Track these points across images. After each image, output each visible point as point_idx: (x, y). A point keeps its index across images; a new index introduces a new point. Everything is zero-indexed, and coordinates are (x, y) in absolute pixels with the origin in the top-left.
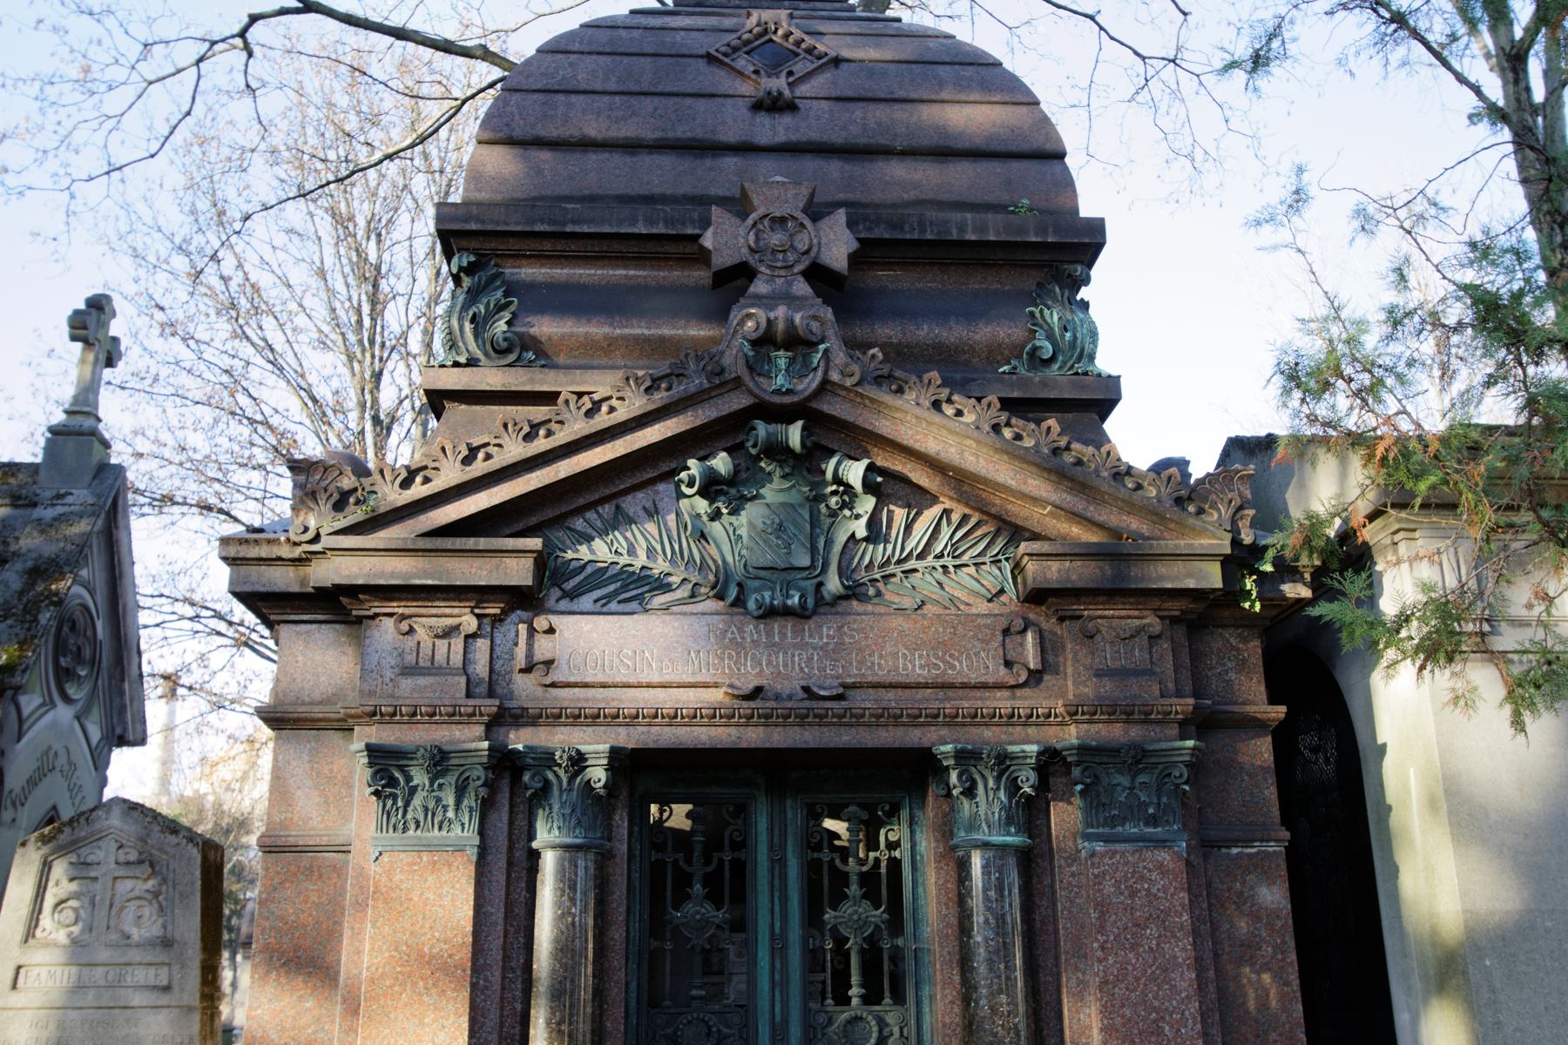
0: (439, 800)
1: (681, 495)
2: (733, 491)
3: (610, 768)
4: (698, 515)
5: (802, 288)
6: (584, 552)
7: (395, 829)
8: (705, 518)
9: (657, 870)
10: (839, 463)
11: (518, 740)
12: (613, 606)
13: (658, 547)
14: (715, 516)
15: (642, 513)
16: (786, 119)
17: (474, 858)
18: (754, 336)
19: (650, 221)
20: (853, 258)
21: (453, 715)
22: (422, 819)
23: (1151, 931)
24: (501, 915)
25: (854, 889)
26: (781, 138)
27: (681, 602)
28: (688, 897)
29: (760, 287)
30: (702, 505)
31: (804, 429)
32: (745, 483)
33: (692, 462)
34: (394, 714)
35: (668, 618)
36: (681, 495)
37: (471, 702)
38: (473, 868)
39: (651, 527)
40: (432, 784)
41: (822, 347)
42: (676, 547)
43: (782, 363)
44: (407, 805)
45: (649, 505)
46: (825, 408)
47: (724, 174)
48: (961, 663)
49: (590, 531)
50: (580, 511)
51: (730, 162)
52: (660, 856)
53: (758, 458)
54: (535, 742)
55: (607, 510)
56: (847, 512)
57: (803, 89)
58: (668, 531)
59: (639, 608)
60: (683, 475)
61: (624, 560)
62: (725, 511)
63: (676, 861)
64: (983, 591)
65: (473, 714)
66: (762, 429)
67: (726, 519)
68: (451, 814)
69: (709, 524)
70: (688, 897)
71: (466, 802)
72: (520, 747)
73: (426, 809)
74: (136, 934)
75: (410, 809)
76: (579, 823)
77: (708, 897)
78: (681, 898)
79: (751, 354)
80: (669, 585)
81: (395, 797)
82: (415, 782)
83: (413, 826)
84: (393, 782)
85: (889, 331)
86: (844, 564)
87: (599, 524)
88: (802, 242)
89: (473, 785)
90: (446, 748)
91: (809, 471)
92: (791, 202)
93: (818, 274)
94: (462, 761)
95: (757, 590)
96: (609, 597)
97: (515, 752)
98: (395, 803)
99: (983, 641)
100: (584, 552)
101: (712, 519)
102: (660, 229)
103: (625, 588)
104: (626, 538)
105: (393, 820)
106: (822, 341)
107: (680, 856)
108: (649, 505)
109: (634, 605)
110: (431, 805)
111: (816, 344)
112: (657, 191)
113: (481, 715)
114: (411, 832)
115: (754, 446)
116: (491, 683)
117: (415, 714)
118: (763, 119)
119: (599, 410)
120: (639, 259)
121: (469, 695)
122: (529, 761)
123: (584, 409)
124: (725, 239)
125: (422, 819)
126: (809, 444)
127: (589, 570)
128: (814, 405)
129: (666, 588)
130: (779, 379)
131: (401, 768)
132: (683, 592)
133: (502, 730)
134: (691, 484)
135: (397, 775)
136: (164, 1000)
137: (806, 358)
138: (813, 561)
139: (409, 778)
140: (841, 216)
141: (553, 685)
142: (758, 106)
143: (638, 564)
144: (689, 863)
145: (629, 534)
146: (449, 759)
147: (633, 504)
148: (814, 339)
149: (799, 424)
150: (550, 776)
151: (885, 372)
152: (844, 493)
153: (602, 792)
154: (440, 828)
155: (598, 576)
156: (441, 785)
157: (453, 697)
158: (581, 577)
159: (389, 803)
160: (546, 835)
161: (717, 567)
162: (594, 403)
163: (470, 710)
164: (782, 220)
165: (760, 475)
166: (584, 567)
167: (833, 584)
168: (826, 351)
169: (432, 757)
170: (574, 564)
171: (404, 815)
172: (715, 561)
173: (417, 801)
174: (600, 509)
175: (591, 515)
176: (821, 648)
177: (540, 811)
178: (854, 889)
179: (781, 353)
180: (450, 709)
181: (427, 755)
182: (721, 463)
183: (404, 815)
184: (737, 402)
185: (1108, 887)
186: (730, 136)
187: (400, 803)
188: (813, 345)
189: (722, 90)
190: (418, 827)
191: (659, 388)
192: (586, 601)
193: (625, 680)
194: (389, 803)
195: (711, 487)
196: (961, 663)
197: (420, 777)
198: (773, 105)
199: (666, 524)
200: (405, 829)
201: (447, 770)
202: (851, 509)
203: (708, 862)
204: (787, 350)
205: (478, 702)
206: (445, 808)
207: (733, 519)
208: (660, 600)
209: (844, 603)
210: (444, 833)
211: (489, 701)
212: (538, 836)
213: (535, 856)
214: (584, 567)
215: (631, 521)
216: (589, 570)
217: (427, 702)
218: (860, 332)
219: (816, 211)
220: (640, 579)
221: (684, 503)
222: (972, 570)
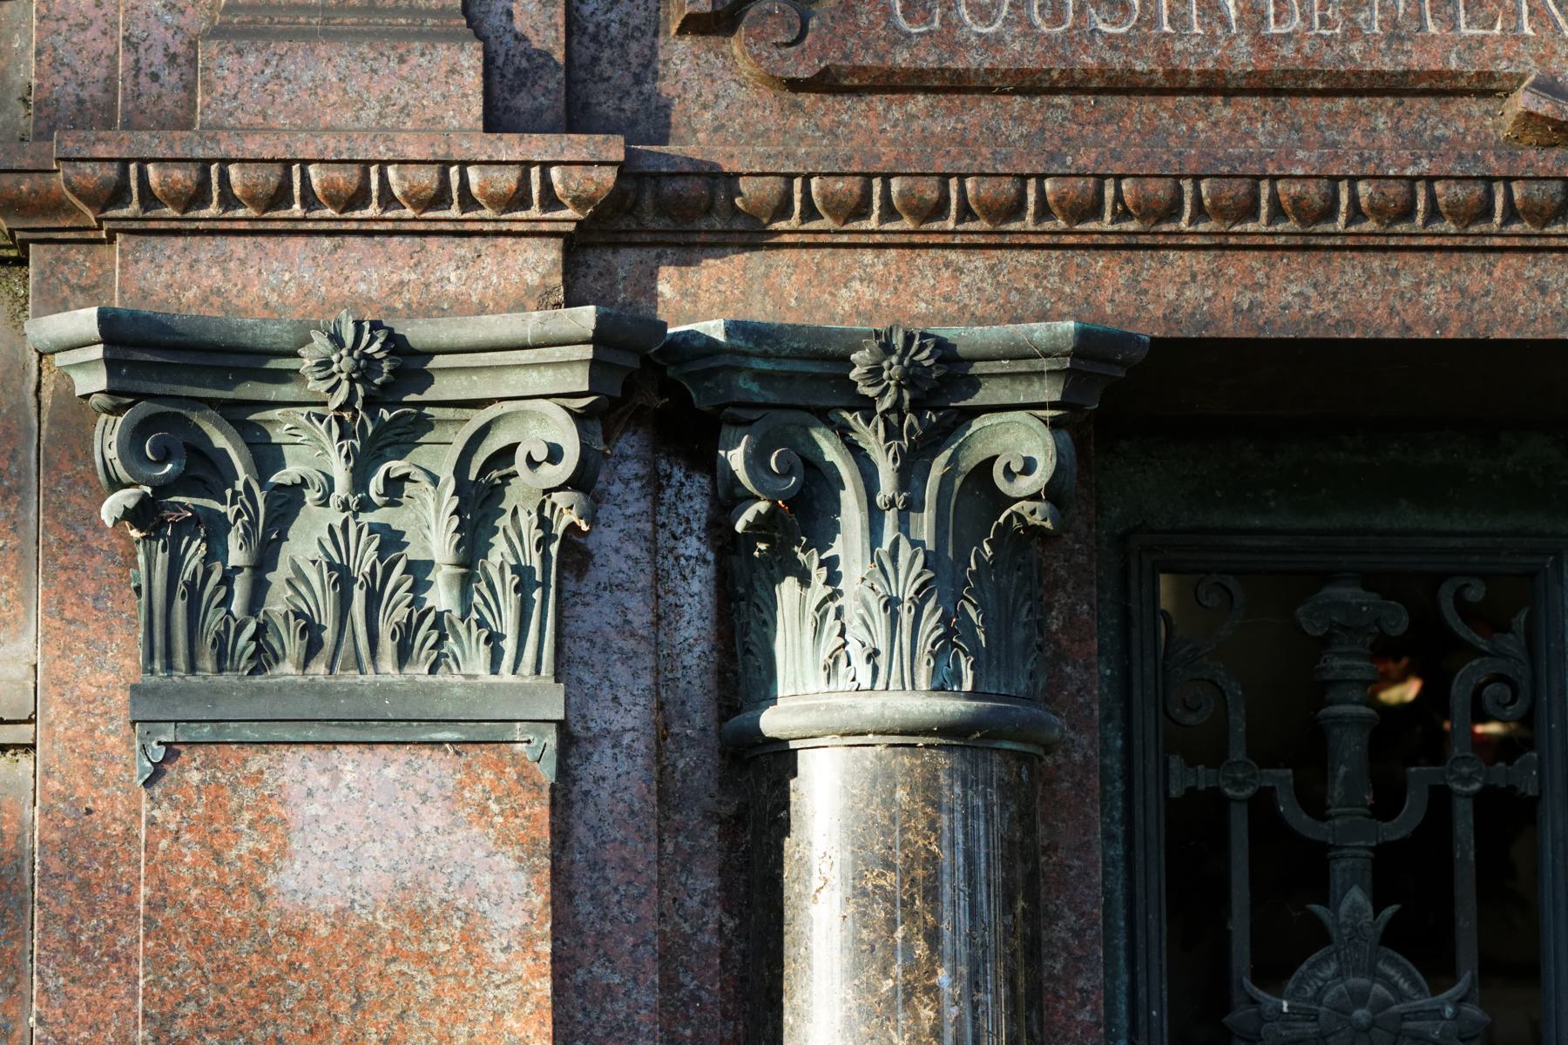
0: (391, 541)
3: (1067, 422)
7: (223, 658)
9: (1194, 832)
11: (701, 300)
17: (547, 772)
21: (440, 199)
22: (328, 621)
24: (646, 996)
25: (1353, 904)
28: (1319, 936)
34: (199, 197)
37: (511, 147)
38: (542, 810)
40: (359, 481)
44: (264, 560)
52: (1203, 778)
54: (760, 312)
63: (1262, 803)
65: (519, 199)
68: (442, 596)
70: (1319, 936)
71: (498, 552)
72: (714, 329)
73: (343, 578)
75: (278, 578)
76: (952, 634)
77: (1393, 937)
81: (215, 530)
82: (288, 474)
83: (294, 647)
84: (206, 471)
89: (522, 492)
90: (419, 333)
94: (479, 387)
97: (694, 349)
98: (216, 551)
105: (213, 621)
107: (1281, 778)
110: (365, 559)
113: (550, 200)
114: (287, 669)
116: (577, 72)
117: (281, 197)
121: (495, 120)
122: (747, 386)
125: (328, 621)
131: (238, 415)
133: (625, 261)
135: (219, 440)
139: (266, 456)
141: (826, 83)
144: (1316, 806)
146: (427, 379)
150: (830, 450)
153: (1039, 515)
154: (404, 655)
156: (395, 486)
157: (431, 126)
159: (195, 552)
160: (815, 681)
163: (507, 180)
169: (365, 368)
171: (256, 600)
173: (305, 543)
177: (788, 590)
178: (1353, 904)
180: (427, 178)
181: (343, 364)
183: (256, 600)
187: (237, 555)
190: (313, 647)
194: (195, 552)
197: (313, 453)
200: (264, 657)
201: (427, 424)
203: (1387, 805)
205: (538, 146)
206: (420, 572)
210: (419, 671)
211: (578, 146)
212: (783, 687)
213: (779, 760)
217: (332, 146)
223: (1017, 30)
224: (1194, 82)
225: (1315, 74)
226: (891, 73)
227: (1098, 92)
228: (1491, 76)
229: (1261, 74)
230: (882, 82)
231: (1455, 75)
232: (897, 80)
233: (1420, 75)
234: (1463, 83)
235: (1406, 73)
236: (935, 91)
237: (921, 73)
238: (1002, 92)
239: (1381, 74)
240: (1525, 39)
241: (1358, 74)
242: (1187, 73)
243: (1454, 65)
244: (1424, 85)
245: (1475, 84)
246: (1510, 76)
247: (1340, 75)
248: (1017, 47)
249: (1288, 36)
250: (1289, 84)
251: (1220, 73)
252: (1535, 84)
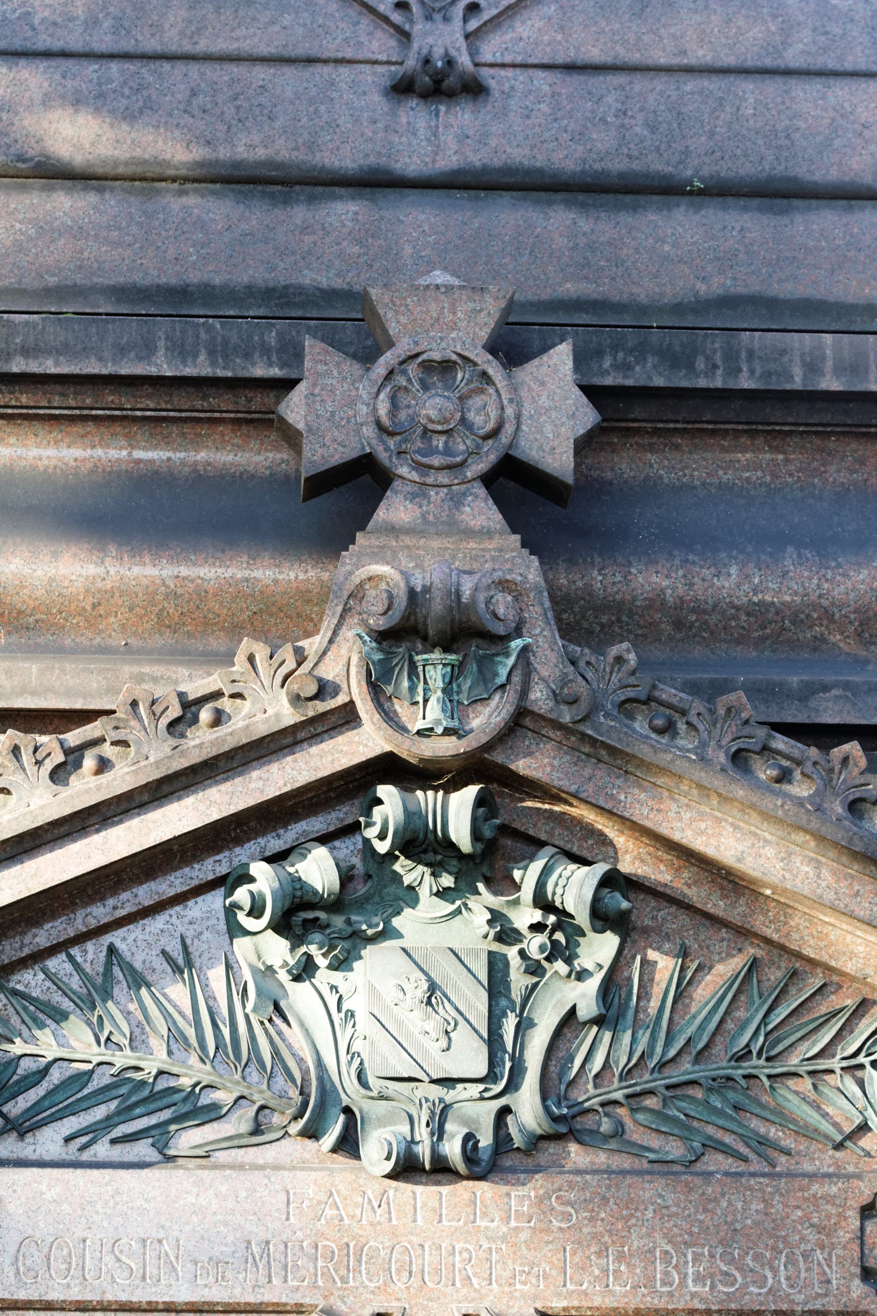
1: (235, 930)
2: (338, 921)
4: (270, 968)
5: (481, 512)
6: (46, 1044)
8: (283, 976)
10: (546, 872)
12: (102, 1150)
13: (191, 1033)
14: (305, 971)
15: (160, 964)
16: (461, 117)
18: (382, 623)
19: (182, 350)
26: (448, 160)
27: (233, 1142)
29: (395, 509)
30: (277, 950)
31: (480, 802)
32: (361, 904)
33: (260, 870)
35: (206, 1174)
36: (235, 930)
39: (178, 993)
41: (516, 644)
42: (226, 1032)
43: (436, 676)
45: (175, 949)
46: (523, 766)
47: (327, 242)
48: (775, 1271)
49: (58, 998)
50: (38, 957)
51: (345, 211)
53: (390, 857)
55: (92, 954)
56: (560, 966)
58: (210, 998)
59: (152, 1155)
60: (242, 895)
61: (122, 1059)
62: (321, 962)
64: (826, 1127)
67: (324, 976)
69: (292, 987)
79: (378, 656)
80: (214, 1106)
85: (653, 579)
86: (553, 1069)
87: (75, 983)
88: (483, 415)
91: (488, 882)
92: (465, 330)
93: (515, 483)
95: (383, 1122)
96: (95, 1131)
99: (819, 1229)
100: (46, 1044)
101: (297, 979)
102: (200, 367)
103: (125, 1113)
104: (127, 1014)
106: (518, 632)
108: (175, 949)
109: (143, 1149)
111: (506, 639)
112: (194, 277)
115: (382, 837)
118: (414, 115)
119: (78, 765)
120: (155, 424)
123: (49, 765)
124: (332, 408)
126: (488, 832)
127: (56, 1076)
128: (498, 757)
129: (212, 1113)
132: (238, 1123)
134: (256, 911)
137: (485, 674)
138: (493, 1062)
140: (561, 356)
142: (403, 88)
143: (151, 1067)
145: (133, 1007)
147: (137, 943)
148: (501, 630)
149: (471, 792)
151: (641, 692)
152: (556, 928)
155: (74, 1091)
158: (40, 1091)
161: (305, 1073)
162: (68, 752)
164: (446, 367)
165: (392, 889)
166: (44, 1072)
167: (528, 1109)
168: (525, 649)
170: (26, 1065)
172: (300, 1061)
174: (75, 951)
175: (58, 964)
176: (504, 1239)
179: (436, 655)
182: (318, 870)
186: (344, 156)
189: (330, 48)
191: (195, 720)
192: (49, 1141)
193: (123, 1297)
195: (297, 916)
196: (775, 1271)
198: (437, 85)
199: (205, 986)
202: (568, 961)
204: (446, 650)
207: (337, 977)
208: (189, 1139)
209: (553, 1147)
214: (44, 1072)
215: (138, 981)
216: (56, 1076)
218: (601, 579)
219: (513, 344)
220: (153, 1096)
221: (242, 945)
222: (806, 1084)
223: (77, 1281)
224: (161, 1307)
225: (218, 1303)
226: (16, 1302)
227: (116, 1310)
228: (302, 1305)
229: (193, 1303)
230: (12, 1306)
231: (285, 1305)
232: (19, 1305)
233: (267, 1304)
234: (289, 1308)
235: (261, 1304)
236: (39, 1309)
237: (30, 1302)
238: (70, 1310)
239: (249, 1304)
240: (319, 1287)
241: (238, 1304)
242: (157, 1303)
243: (284, 1300)
244: (270, 1309)
245: (295, 1309)
246: (311, 1305)
247: (229, 1304)
248: (77, 1289)
249: (206, 1286)
250: (206, 1308)
251: (173, 1303)
252: (322, 1311)
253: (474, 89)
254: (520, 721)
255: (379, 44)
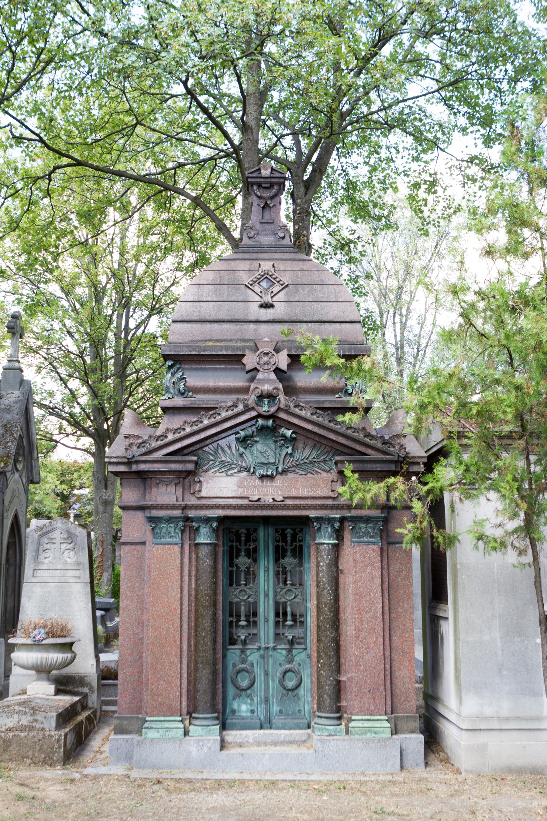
5: (273, 376)
12: (217, 474)
16: (271, 310)
20: (288, 366)
23: (369, 568)
50: (207, 445)
55: (215, 445)
57: (275, 299)
66: (261, 422)
74: (69, 560)
78: (238, 556)
88: (272, 361)
93: (278, 371)
96: (216, 472)
109: (224, 474)
118: (263, 310)
130: (265, 408)
136: (79, 581)
142: (261, 306)
175: (210, 446)
184: (254, 414)
185: (358, 556)
186: (252, 318)
188: (275, 397)
189: (250, 299)
198: (267, 306)
208: (230, 473)
219: (277, 350)
253: (272, 306)
254: (279, 409)
255: (258, 298)
